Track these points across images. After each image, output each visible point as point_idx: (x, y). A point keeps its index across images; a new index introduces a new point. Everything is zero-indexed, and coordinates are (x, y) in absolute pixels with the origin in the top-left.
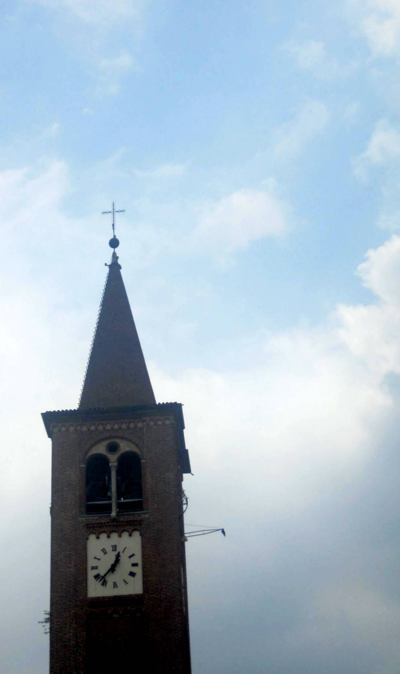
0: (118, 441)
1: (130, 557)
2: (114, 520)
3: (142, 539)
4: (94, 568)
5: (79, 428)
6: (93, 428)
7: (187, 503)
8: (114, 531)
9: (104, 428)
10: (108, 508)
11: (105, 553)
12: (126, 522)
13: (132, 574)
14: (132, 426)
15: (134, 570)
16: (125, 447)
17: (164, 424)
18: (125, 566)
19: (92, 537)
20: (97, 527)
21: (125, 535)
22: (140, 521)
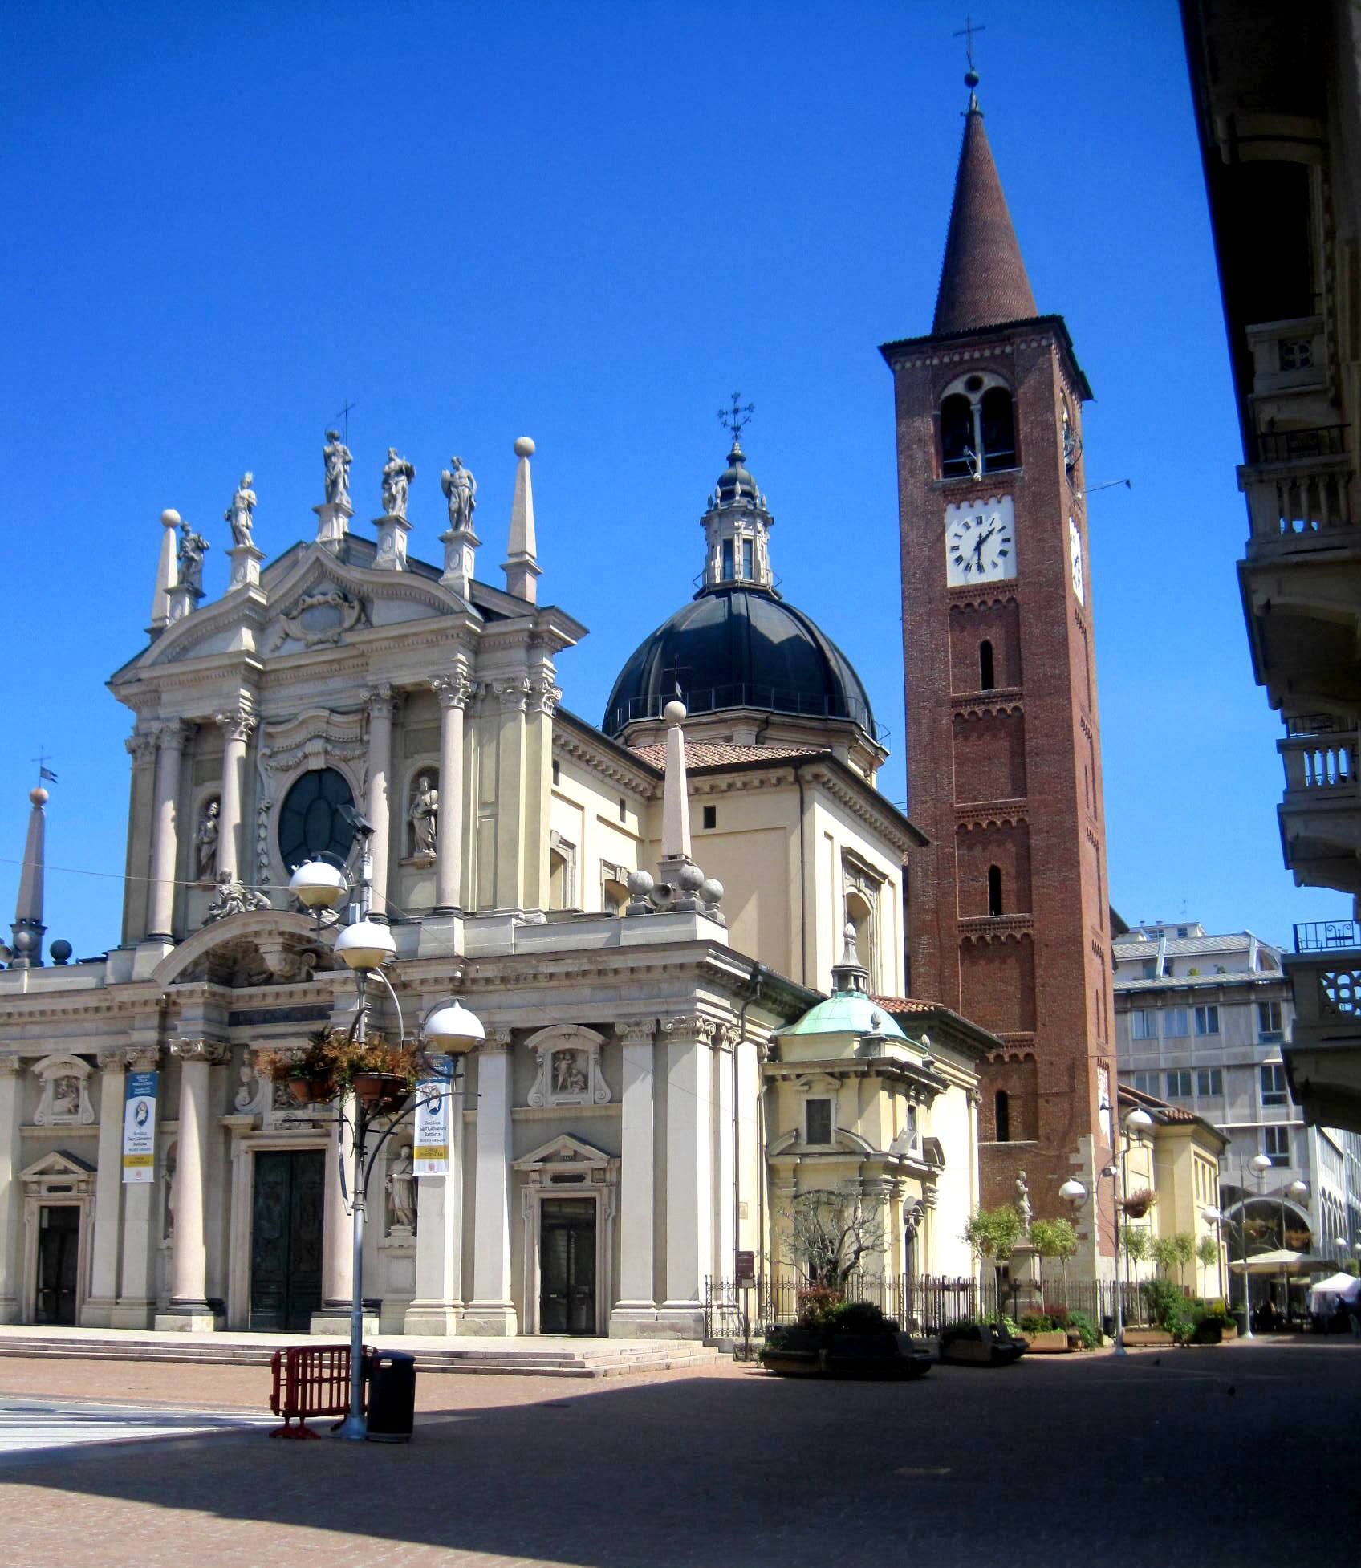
0: (976, 374)
2: (975, 483)
3: (1015, 506)
5: (928, 362)
6: (946, 360)
7: (1081, 447)
8: (979, 498)
9: (961, 359)
13: (1003, 553)
14: (998, 351)
16: (989, 382)
19: (951, 508)
21: (993, 501)
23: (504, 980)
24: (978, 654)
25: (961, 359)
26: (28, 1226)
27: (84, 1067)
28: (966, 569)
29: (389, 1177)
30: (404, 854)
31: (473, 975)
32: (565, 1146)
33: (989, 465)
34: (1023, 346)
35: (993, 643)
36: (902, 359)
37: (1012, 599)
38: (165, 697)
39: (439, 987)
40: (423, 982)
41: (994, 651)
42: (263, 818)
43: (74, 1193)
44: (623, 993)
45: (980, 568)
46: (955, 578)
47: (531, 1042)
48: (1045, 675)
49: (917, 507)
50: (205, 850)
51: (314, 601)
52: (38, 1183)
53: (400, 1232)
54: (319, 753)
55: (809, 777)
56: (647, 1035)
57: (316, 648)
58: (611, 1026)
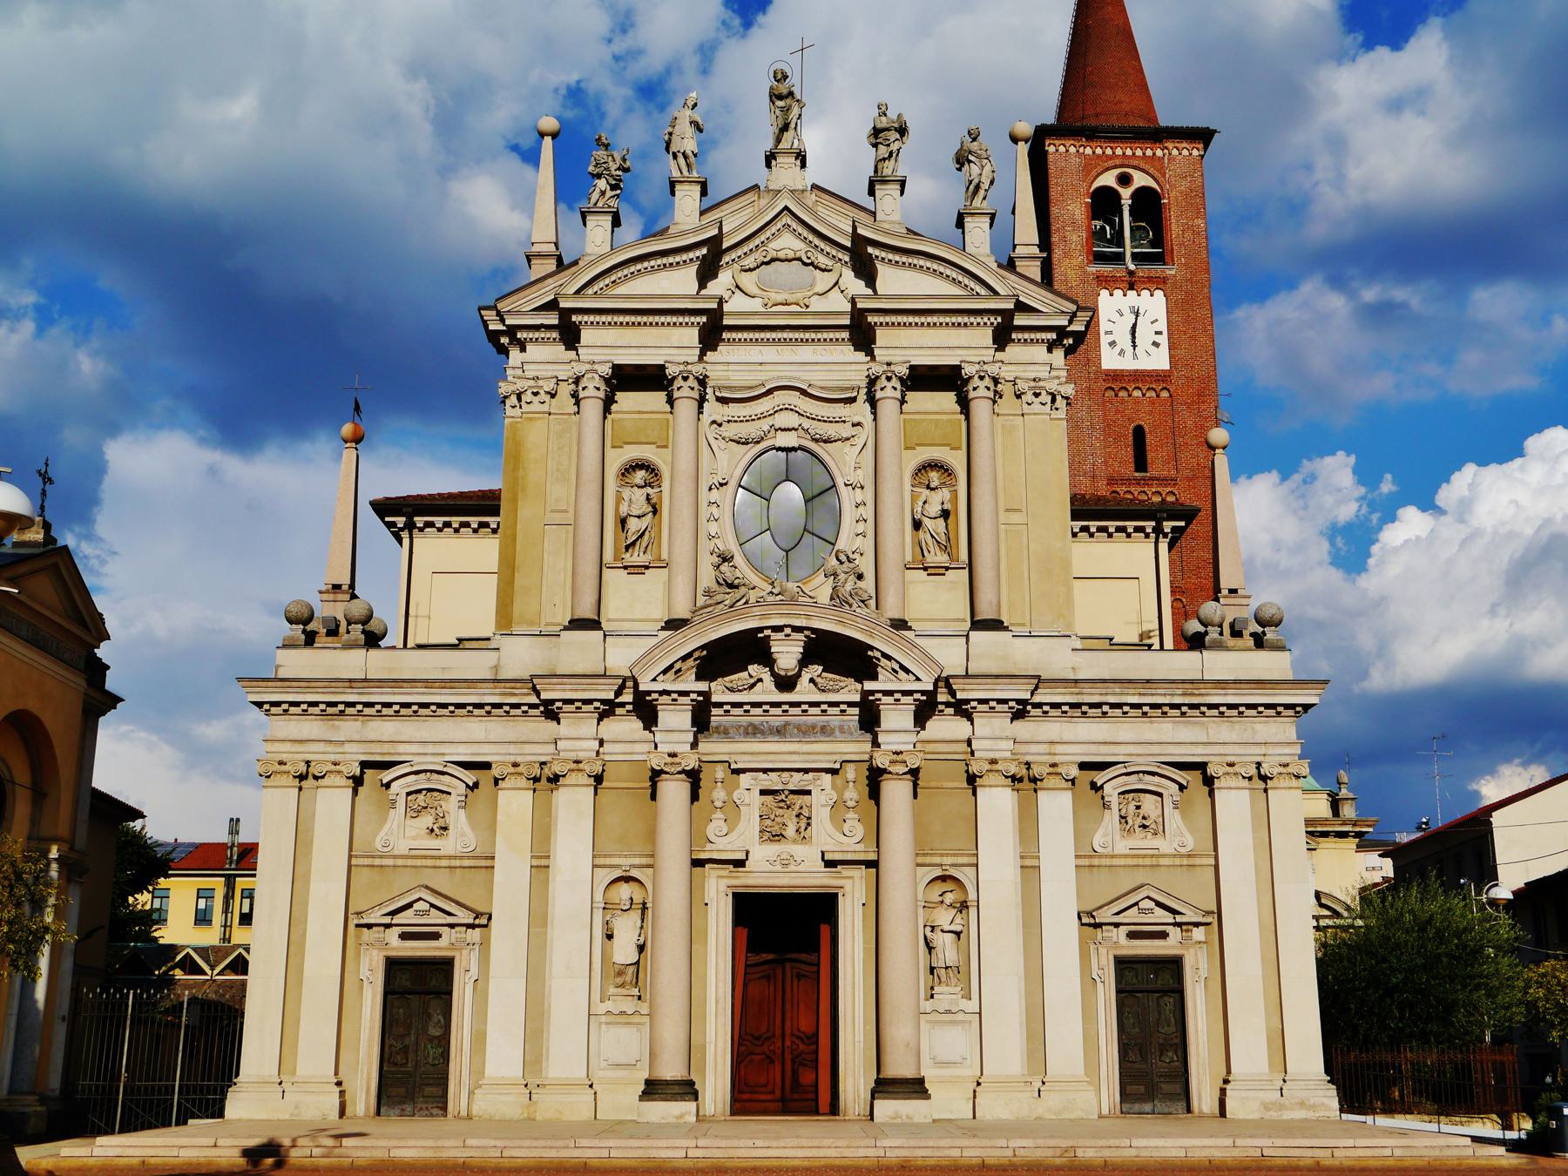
1: (1152, 323)
2: (1131, 273)
4: (1107, 333)
5: (1081, 150)
6: (1099, 151)
9: (1114, 153)
10: (1118, 258)
11: (1122, 315)
12: (1147, 277)
13: (1156, 344)
14: (1149, 153)
15: (1158, 339)
16: (1140, 180)
17: (1191, 154)
18: (1145, 335)
19: (1104, 293)
20: (1109, 281)
21: (1146, 293)
22: (1164, 278)
23: (1074, 706)
24: (1131, 439)
25: (1114, 153)
26: (365, 982)
27: (470, 777)
28: (1120, 354)
29: (928, 929)
30: (909, 558)
31: (1037, 699)
32: (1148, 897)
33: (1135, 256)
34: (1175, 152)
35: (1147, 430)
36: (1057, 142)
37: (1163, 389)
38: (586, 336)
39: (1000, 707)
40: (981, 701)
41: (1148, 436)
42: (715, 495)
43: (443, 942)
44: (1210, 731)
45: (1135, 356)
46: (1110, 360)
47: (1100, 778)
48: (1198, 464)
49: (1072, 287)
50: (634, 525)
51: (781, 255)
52: (388, 926)
53: (947, 995)
54: (796, 430)
55: (1167, 530)
56: (1244, 777)
57: (775, 309)
58: (1201, 767)
